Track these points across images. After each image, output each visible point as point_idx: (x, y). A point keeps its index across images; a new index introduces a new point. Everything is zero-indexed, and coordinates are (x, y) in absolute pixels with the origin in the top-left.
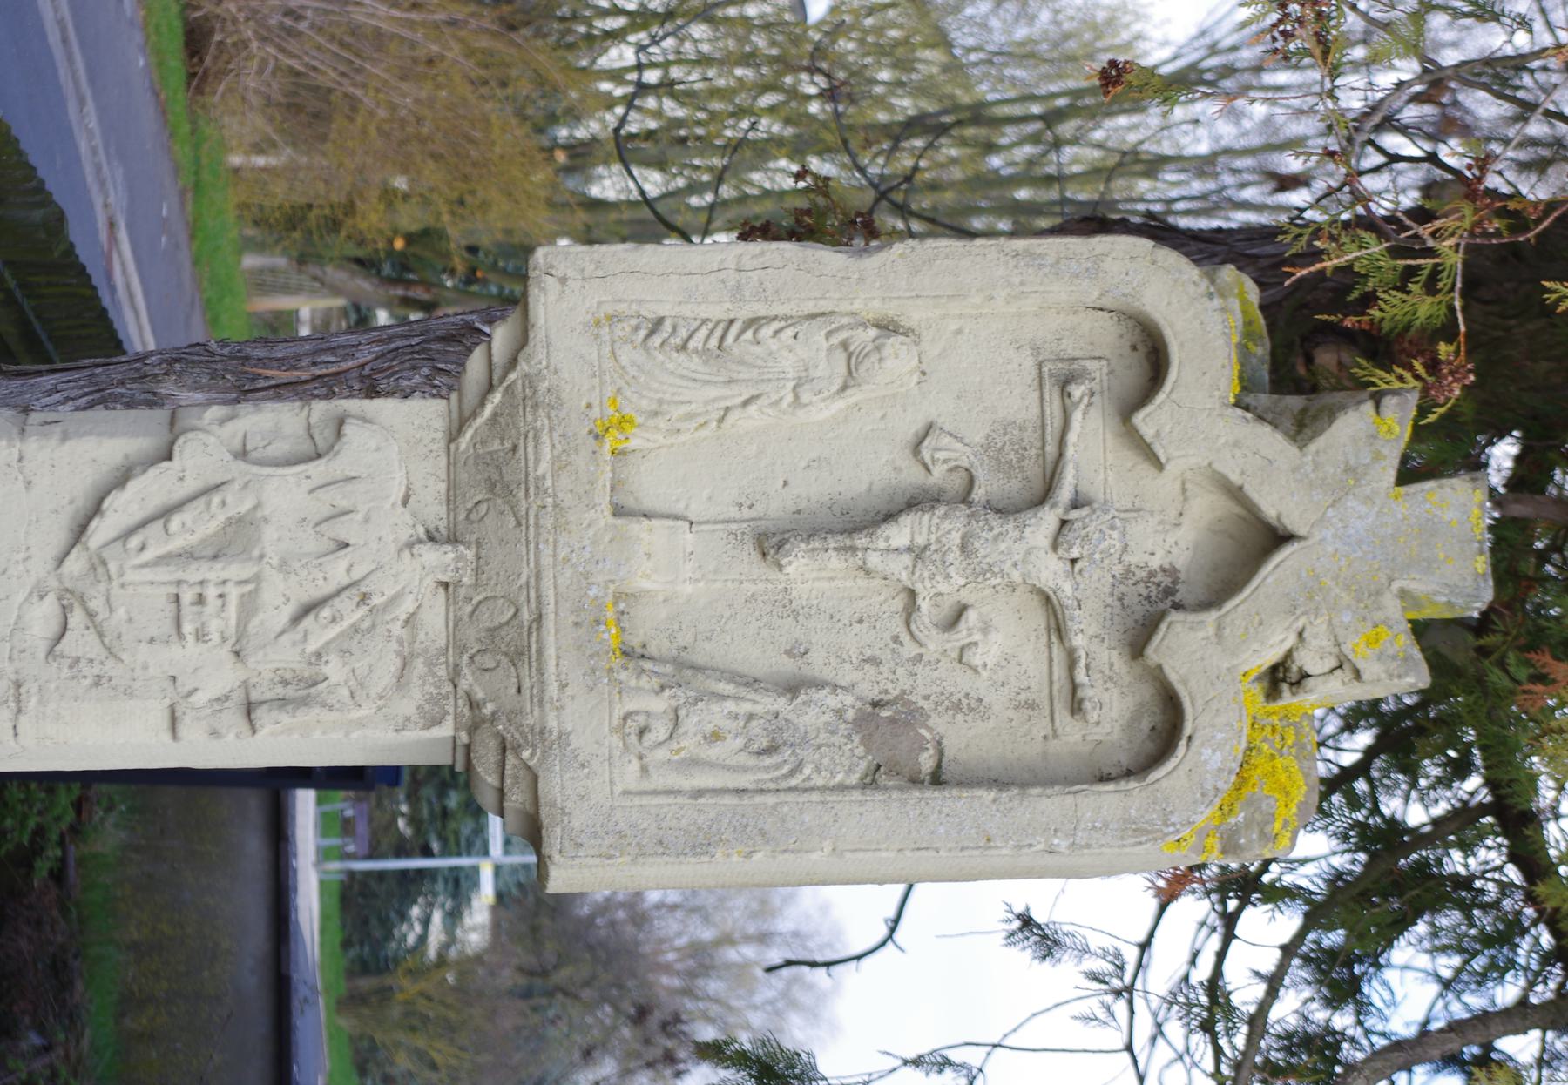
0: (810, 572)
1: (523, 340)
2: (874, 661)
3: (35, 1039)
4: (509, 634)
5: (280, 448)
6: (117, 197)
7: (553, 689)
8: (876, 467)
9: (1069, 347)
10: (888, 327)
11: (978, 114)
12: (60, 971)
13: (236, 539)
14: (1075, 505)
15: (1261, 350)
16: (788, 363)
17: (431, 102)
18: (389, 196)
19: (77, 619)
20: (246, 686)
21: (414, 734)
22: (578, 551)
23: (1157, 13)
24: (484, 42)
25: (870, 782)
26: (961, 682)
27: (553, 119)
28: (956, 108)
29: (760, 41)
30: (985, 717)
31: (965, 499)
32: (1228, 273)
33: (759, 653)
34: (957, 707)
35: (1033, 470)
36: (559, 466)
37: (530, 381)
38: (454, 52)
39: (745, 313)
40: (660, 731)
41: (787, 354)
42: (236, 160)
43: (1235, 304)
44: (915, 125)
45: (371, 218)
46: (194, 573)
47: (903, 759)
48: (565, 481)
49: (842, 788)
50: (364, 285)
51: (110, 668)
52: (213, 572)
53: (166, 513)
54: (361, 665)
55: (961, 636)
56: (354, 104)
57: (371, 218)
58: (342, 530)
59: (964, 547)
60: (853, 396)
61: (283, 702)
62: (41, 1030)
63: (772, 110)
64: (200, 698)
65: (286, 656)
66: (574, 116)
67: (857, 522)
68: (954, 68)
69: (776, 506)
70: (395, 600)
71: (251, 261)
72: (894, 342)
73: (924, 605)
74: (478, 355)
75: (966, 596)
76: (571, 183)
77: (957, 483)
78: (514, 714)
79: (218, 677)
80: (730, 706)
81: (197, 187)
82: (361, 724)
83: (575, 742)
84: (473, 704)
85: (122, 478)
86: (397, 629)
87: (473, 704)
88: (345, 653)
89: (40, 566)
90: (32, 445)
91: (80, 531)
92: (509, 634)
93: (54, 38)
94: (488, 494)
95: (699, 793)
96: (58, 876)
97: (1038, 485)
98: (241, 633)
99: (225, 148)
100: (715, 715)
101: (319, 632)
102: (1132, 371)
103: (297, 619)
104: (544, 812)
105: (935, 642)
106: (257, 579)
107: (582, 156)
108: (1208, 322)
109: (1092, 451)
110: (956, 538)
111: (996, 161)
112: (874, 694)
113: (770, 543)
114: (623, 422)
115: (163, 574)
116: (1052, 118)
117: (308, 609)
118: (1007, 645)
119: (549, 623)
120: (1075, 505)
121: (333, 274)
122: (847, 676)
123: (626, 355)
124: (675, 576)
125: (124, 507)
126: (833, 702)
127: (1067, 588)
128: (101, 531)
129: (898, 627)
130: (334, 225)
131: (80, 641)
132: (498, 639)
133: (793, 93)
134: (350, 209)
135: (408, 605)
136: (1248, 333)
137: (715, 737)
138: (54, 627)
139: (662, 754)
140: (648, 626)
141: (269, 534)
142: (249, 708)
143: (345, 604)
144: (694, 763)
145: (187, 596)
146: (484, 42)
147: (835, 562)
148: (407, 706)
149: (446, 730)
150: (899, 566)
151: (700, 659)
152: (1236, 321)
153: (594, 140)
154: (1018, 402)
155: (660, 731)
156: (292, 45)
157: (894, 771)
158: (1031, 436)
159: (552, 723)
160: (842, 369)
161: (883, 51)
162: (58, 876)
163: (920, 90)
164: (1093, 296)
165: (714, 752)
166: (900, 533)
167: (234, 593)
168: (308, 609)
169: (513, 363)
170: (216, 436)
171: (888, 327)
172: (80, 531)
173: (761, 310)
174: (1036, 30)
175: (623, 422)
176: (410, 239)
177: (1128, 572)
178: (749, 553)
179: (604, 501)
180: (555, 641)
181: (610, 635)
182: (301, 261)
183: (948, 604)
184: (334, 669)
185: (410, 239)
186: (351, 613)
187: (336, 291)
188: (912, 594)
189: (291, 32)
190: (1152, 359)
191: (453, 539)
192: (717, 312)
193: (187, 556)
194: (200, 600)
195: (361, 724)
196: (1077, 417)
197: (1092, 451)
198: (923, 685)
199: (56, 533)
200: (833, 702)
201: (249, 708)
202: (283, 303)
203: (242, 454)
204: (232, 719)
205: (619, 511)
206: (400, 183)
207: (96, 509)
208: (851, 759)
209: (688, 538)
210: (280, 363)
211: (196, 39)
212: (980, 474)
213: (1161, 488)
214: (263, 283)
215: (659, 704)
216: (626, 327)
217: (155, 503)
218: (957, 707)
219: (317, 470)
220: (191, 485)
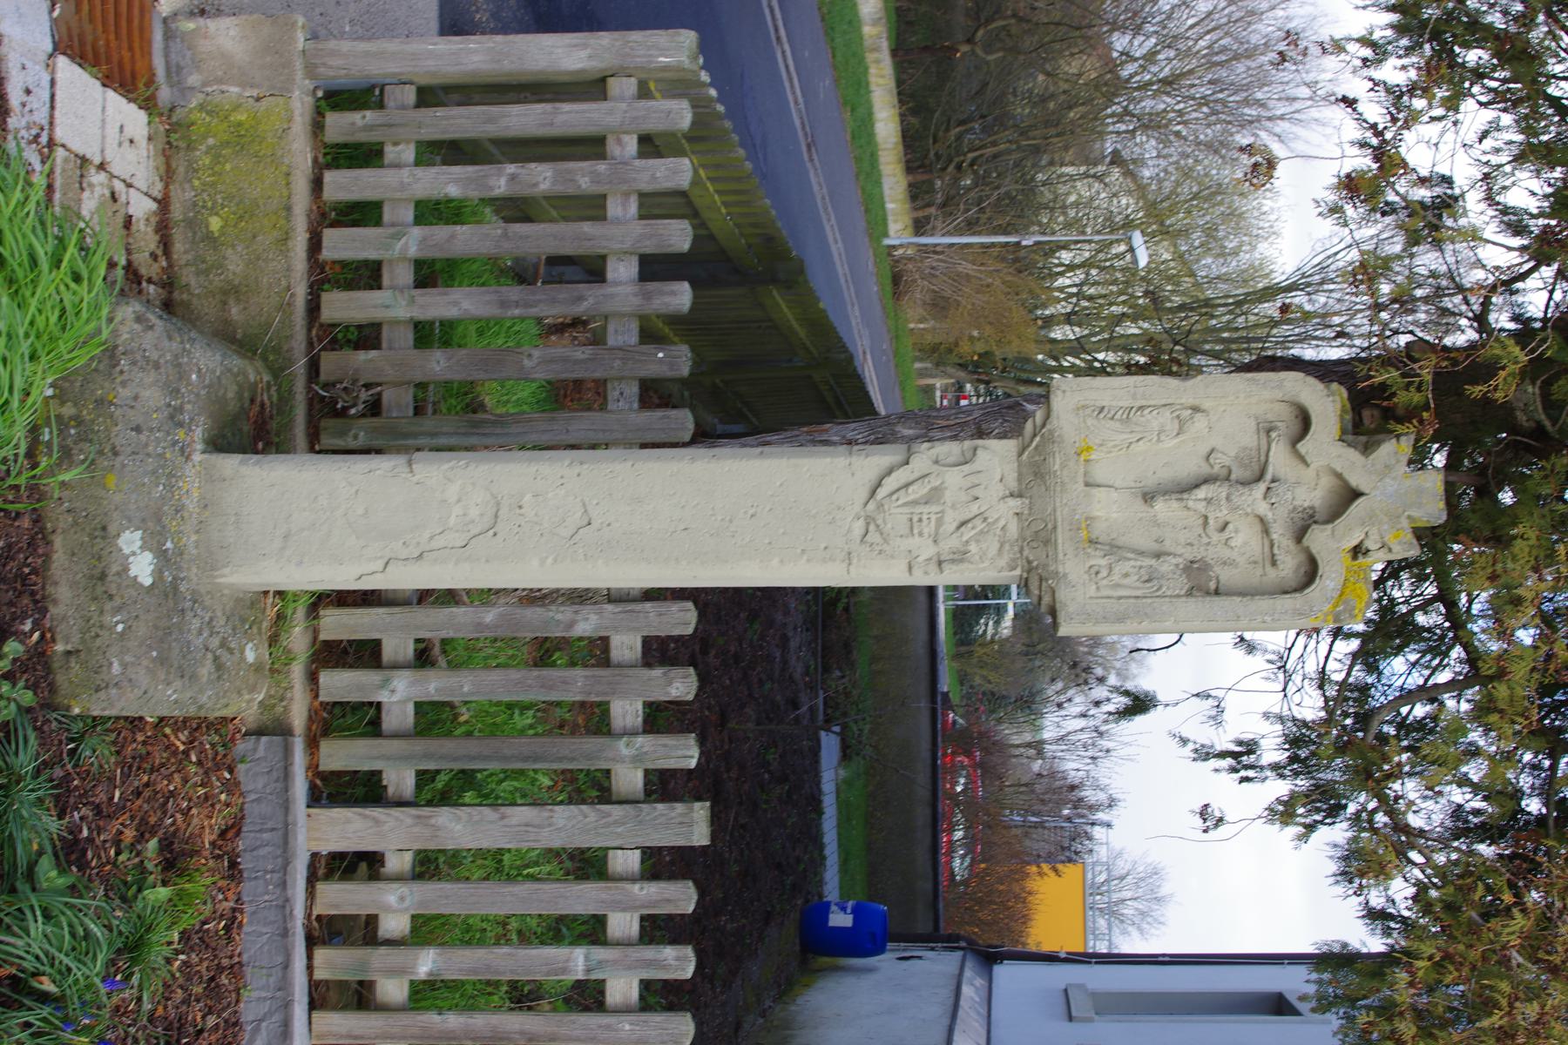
0: (1164, 508)
1: (1048, 416)
2: (1191, 545)
3: (838, 673)
4: (1043, 534)
5: (951, 460)
6: (866, 342)
7: (1061, 556)
8: (1192, 466)
9: (1270, 417)
10: (1196, 409)
11: (1207, 303)
12: (847, 647)
13: (934, 496)
14: (1273, 481)
15: (1348, 417)
16: (1155, 425)
17: (988, 303)
18: (971, 338)
19: (872, 527)
20: (938, 554)
21: (1006, 574)
22: (1069, 501)
23: (1280, 261)
24: (1009, 278)
25: (1189, 594)
26: (1226, 553)
27: (1036, 307)
28: (1198, 301)
29: (1119, 275)
30: (1236, 566)
31: (1227, 479)
32: (1335, 386)
33: (1145, 542)
34: (1225, 563)
35: (1256, 468)
36: (1063, 466)
37: (1051, 432)
38: (998, 282)
39: (1138, 404)
40: (1104, 573)
41: (1155, 421)
42: (912, 326)
43: (1337, 398)
44: (1182, 307)
45: (965, 348)
46: (918, 509)
47: (1203, 585)
48: (1065, 472)
49: (1178, 596)
50: (962, 374)
51: (885, 547)
52: (926, 509)
53: (907, 485)
54: (984, 546)
55: (1226, 534)
56: (958, 304)
57: (965, 348)
58: (975, 492)
59: (1228, 498)
60: (1181, 438)
61: (953, 561)
62: (840, 669)
63: (1124, 302)
64: (920, 559)
65: (953, 543)
66: (1044, 306)
67: (1184, 488)
68: (1197, 285)
69: (1151, 482)
70: (998, 520)
71: (918, 365)
72: (1199, 415)
73: (1211, 522)
74: (1030, 422)
75: (1228, 518)
76: (1043, 333)
77: (1224, 472)
78: (1045, 566)
79: (927, 551)
80: (1132, 563)
81: (897, 337)
82: (984, 569)
83: (1070, 577)
84: (1029, 562)
85: (890, 472)
86: (998, 532)
87: (1029, 562)
88: (978, 541)
89: (858, 507)
90: (854, 459)
91: (873, 493)
92: (1043, 534)
93: (842, 281)
94: (1035, 478)
95: (1120, 598)
96: (846, 609)
97: (1257, 473)
98: (937, 534)
99: (908, 321)
100: (1127, 566)
101: (968, 533)
102: (1296, 427)
103: (959, 528)
104: (1058, 606)
105: (1216, 537)
106: (942, 512)
107: (1049, 322)
108: (1326, 404)
109: (1280, 460)
110: (1224, 495)
111: (1214, 322)
112: (1191, 558)
113: (1148, 497)
114: (1089, 448)
115: (906, 510)
116: (1239, 304)
117: (963, 524)
118: (1245, 538)
119: (1059, 530)
120: (1273, 481)
121: (950, 370)
122: (1180, 550)
123: (1090, 422)
124: (1110, 510)
125: (891, 483)
126: (1174, 561)
127: (1270, 515)
128: (881, 493)
129: (1200, 530)
130: (950, 351)
131: (873, 536)
132: (1039, 536)
133: (1132, 296)
134: (957, 345)
135: (1002, 523)
136: (1343, 411)
137: (1126, 575)
138: (863, 531)
139: (1105, 582)
140: (1099, 530)
141: (948, 494)
142: (940, 563)
143: (977, 522)
144: (1118, 586)
145: (915, 519)
146: (1009, 278)
147: (1175, 505)
148: (1003, 562)
149: (1018, 572)
150: (1201, 506)
151: (1120, 543)
152: (1338, 406)
153: (1052, 315)
154: (1249, 438)
155: (1104, 573)
156: (934, 281)
157: (1200, 589)
158: (1254, 453)
159: (1061, 569)
160: (1177, 426)
161: (1170, 279)
162: (846, 609)
163: (1184, 294)
164: (1280, 396)
165: (1126, 581)
166: (1201, 493)
167: (934, 517)
168: (963, 524)
169: (1044, 425)
170: (925, 456)
171: (1196, 409)
172: (873, 493)
173: (1144, 403)
174: (1230, 269)
175: (1089, 448)
176: (980, 355)
177: (1295, 508)
178: (1140, 501)
179: (1081, 480)
180: (1061, 537)
181: (1084, 534)
182: (937, 365)
183: (1221, 521)
184: (973, 548)
185: (980, 355)
186: (980, 526)
187: (951, 377)
188: (1206, 517)
189: (934, 276)
190: (1304, 422)
191: (1020, 496)
192: (1126, 404)
193: (915, 503)
194: (920, 520)
195: (984, 569)
196: (1273, 445)
197: (1280, 460)
198: (1211, 554)
199: (864, 493)
200: (1174, 561)
201: (940, 563)
202: (930, 381)
203: (936, 462)
204: (933, 567)
205: (1087, 485)
206: (975, 333)
207: (879, 485)
208: (1180, 584)
209: (1114, 495)
210: (943, 418)
211: (896, 279)
212: (1234, 469)
213: (1310, 473)
214: (922, 374)
215: (1103, 562)
216: (1088, 411)
217: (903, 481)
218: (1225, 563)
219: (966, 468)
220: (916, 475)
